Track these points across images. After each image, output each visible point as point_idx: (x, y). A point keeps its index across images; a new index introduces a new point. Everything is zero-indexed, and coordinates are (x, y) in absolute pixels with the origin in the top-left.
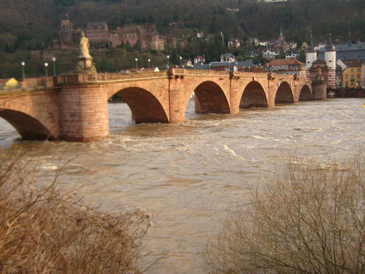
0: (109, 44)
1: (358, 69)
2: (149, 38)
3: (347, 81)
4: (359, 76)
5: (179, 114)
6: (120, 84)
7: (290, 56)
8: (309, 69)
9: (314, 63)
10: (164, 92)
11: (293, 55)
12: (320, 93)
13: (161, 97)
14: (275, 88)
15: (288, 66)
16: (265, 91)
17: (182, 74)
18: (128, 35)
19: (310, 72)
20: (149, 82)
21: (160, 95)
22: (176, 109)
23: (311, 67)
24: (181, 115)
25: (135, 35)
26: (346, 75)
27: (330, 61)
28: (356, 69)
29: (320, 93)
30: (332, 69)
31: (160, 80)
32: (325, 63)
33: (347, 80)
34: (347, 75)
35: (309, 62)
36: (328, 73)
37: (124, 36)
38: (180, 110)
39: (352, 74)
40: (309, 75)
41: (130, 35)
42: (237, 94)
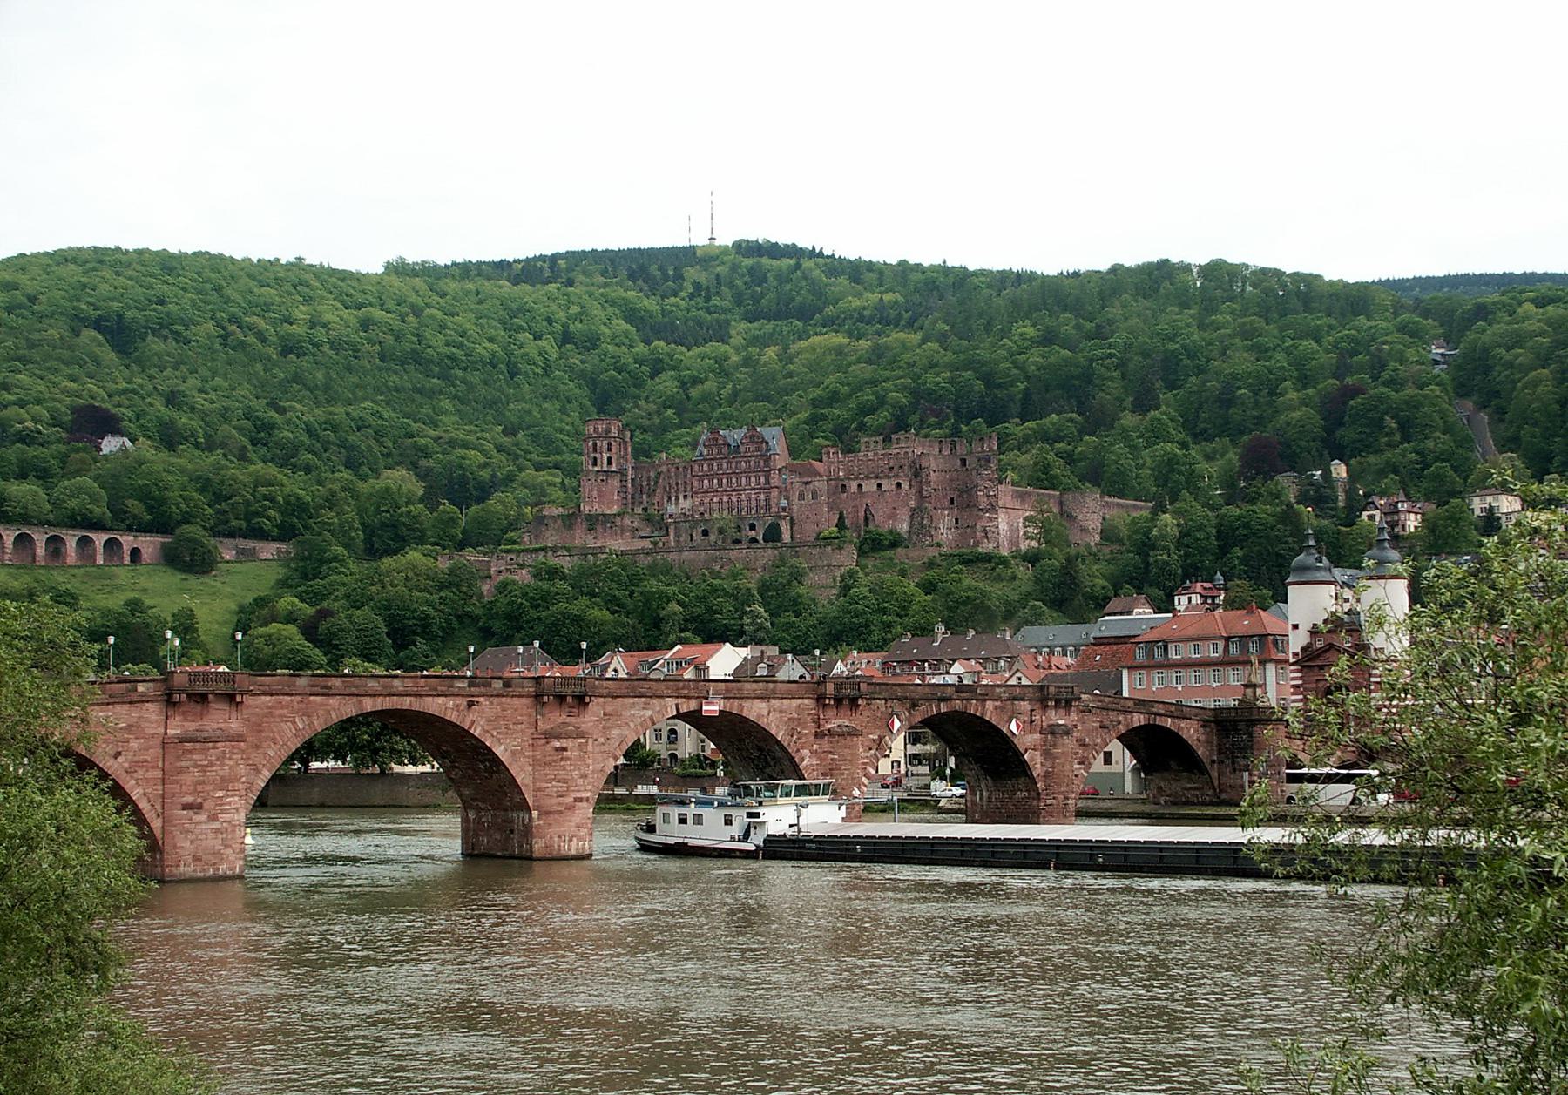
0: (785, 527)
2: (964, 500)
5: (203, 817)
8: (1295, 654)
10: (134, 744)
13: (120, 759)
15: (1221, 644)
17: (222, 687)
18: (870, 486)
21: (117, 755)
22: (189, 799)
23: (1303, 649)
24: (213, 818)
25: (905, 486)
31: (122, 709)
35: (1296, 627)
37: (853, 486)
38: (208, 805)
41: (879, 485)
42: (568, 759)
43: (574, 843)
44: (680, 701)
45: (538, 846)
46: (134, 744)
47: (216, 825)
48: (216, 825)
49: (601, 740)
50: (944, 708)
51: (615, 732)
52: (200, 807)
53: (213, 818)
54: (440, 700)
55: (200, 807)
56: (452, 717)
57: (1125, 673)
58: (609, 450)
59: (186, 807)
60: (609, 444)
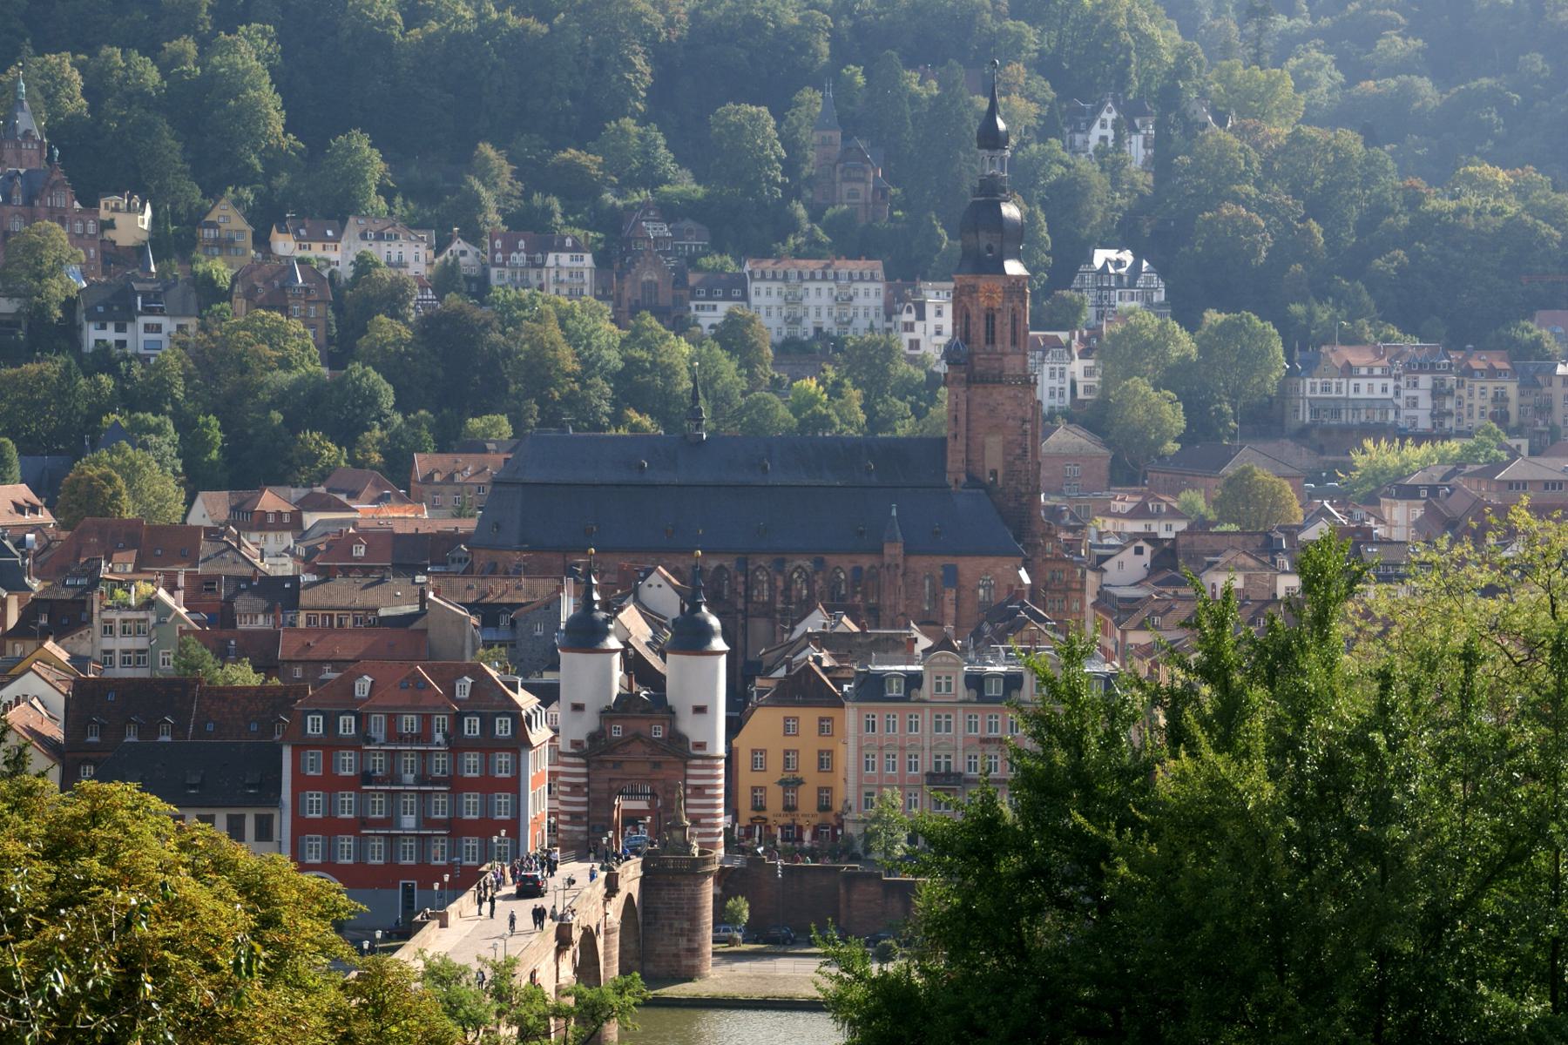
1: (821, 720)
3: (762, 789)
4: (825, 761)
7: (120, 328)
8: (575, 744)
9: (608, 714)
11: (148, 328)
12: (686, 925)
19: (587, 765)
23: (593, 737)
26: (754, 752)
27: (700, 710)
28: (808, 717)
29: (686, 925)
30: (707, 752)
32: (671, 713)
33: (758, 779)
34: (763, 752)
35: (578, 708)
36: (687, 777)
39: (791, 743)
40: (583, 780)
57: (287, 753)
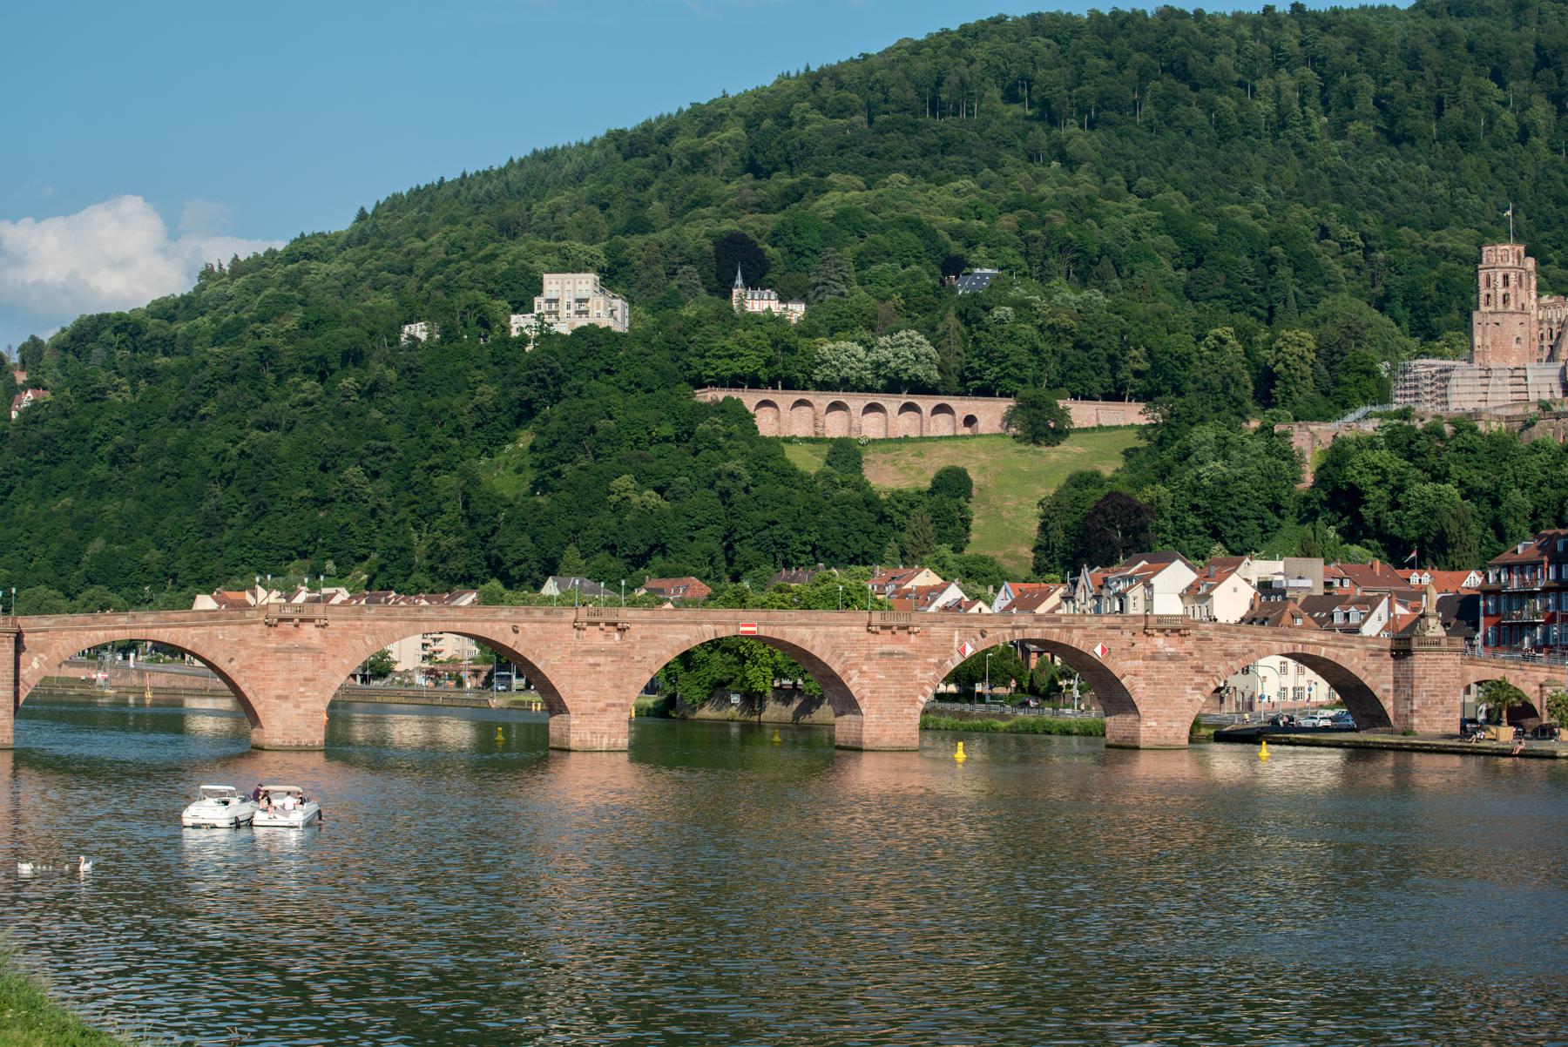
5: (289, 705)
6: (101, 633)
14: (934, 660)
16: (837, 669)
20: (192, 631)
21: (231, 660)
43: (605, 741)
44: (718, 627)
45: (574, 742)
46: (244, 653)
47: (301, 711)
48: (301, 711)
49: (637, 658)
50: (1018, 635)
51: (652, 652)
52: (287, 698)
53: (297, 706)
54: (488, 625)
55: (287, 698)
56: (499, 639)
58: (1506, 284)
59: (278, 697)
60: (1506, 277)
